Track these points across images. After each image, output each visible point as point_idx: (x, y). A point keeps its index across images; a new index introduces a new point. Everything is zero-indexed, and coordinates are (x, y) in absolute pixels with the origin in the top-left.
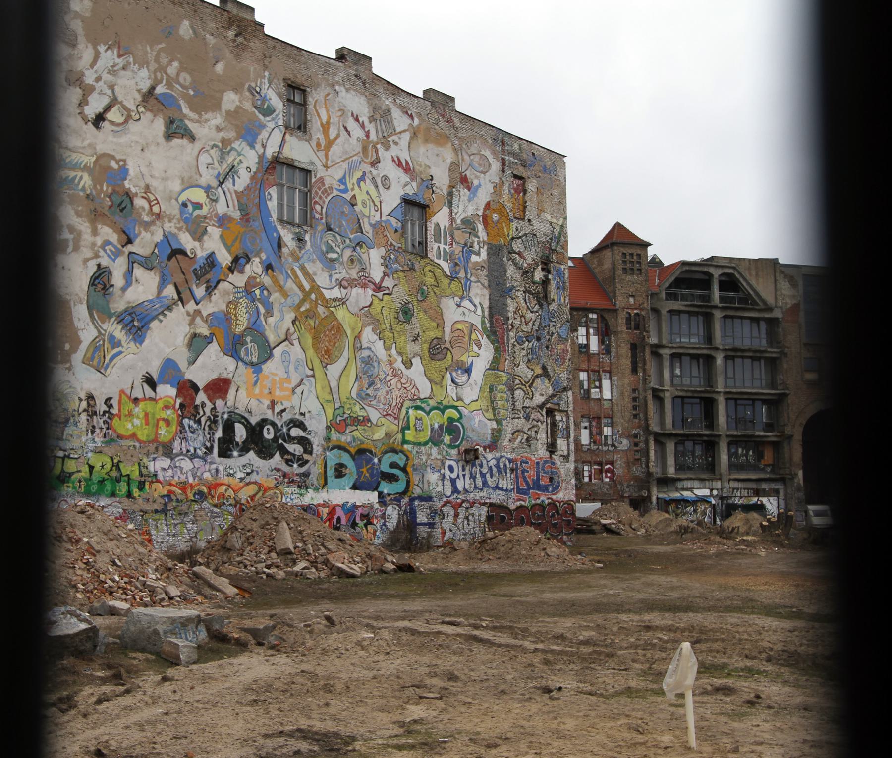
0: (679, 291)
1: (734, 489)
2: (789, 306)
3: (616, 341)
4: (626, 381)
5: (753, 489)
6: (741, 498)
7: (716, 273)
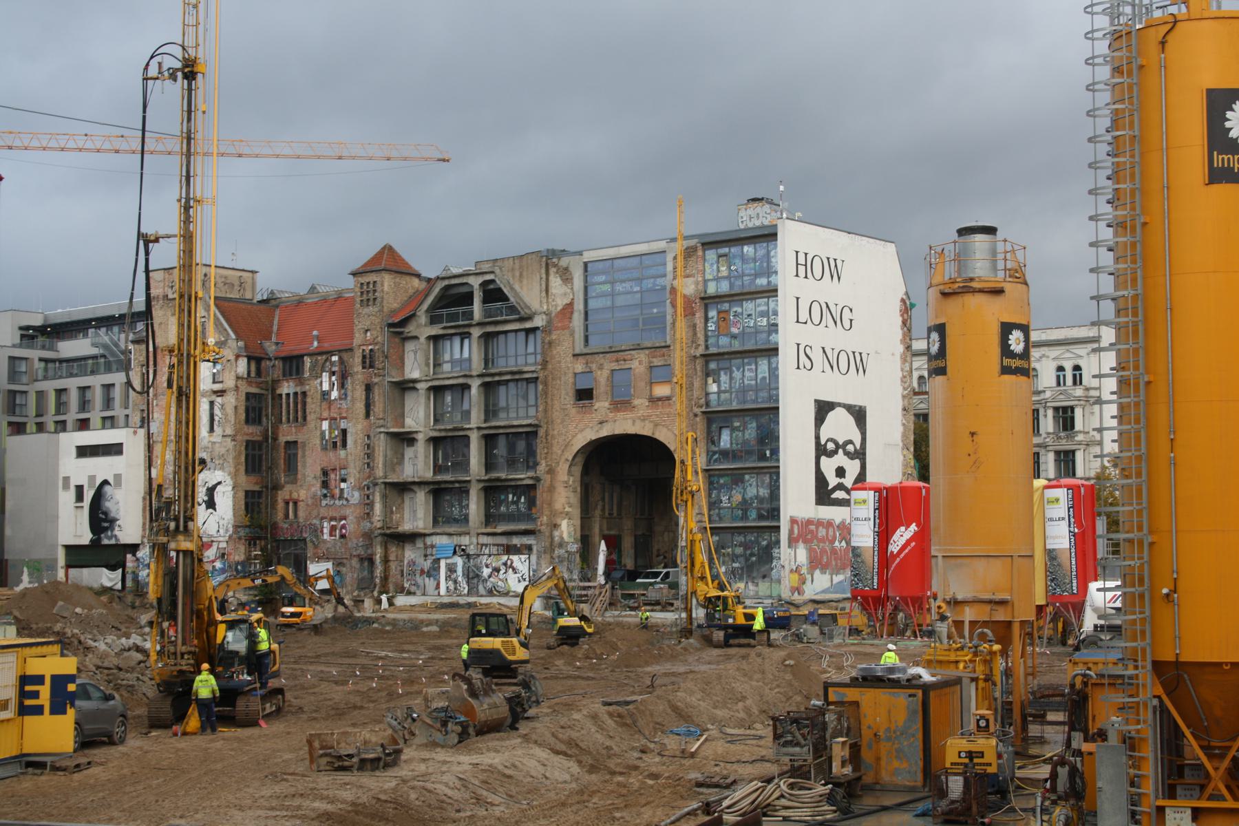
0: (445, 311)
1: (482, 545)
2: (559, 308)
3: (353, 383)
4: (360, 427)
5: (503, 545)
6: (490, 556)
7: (475, 282)
